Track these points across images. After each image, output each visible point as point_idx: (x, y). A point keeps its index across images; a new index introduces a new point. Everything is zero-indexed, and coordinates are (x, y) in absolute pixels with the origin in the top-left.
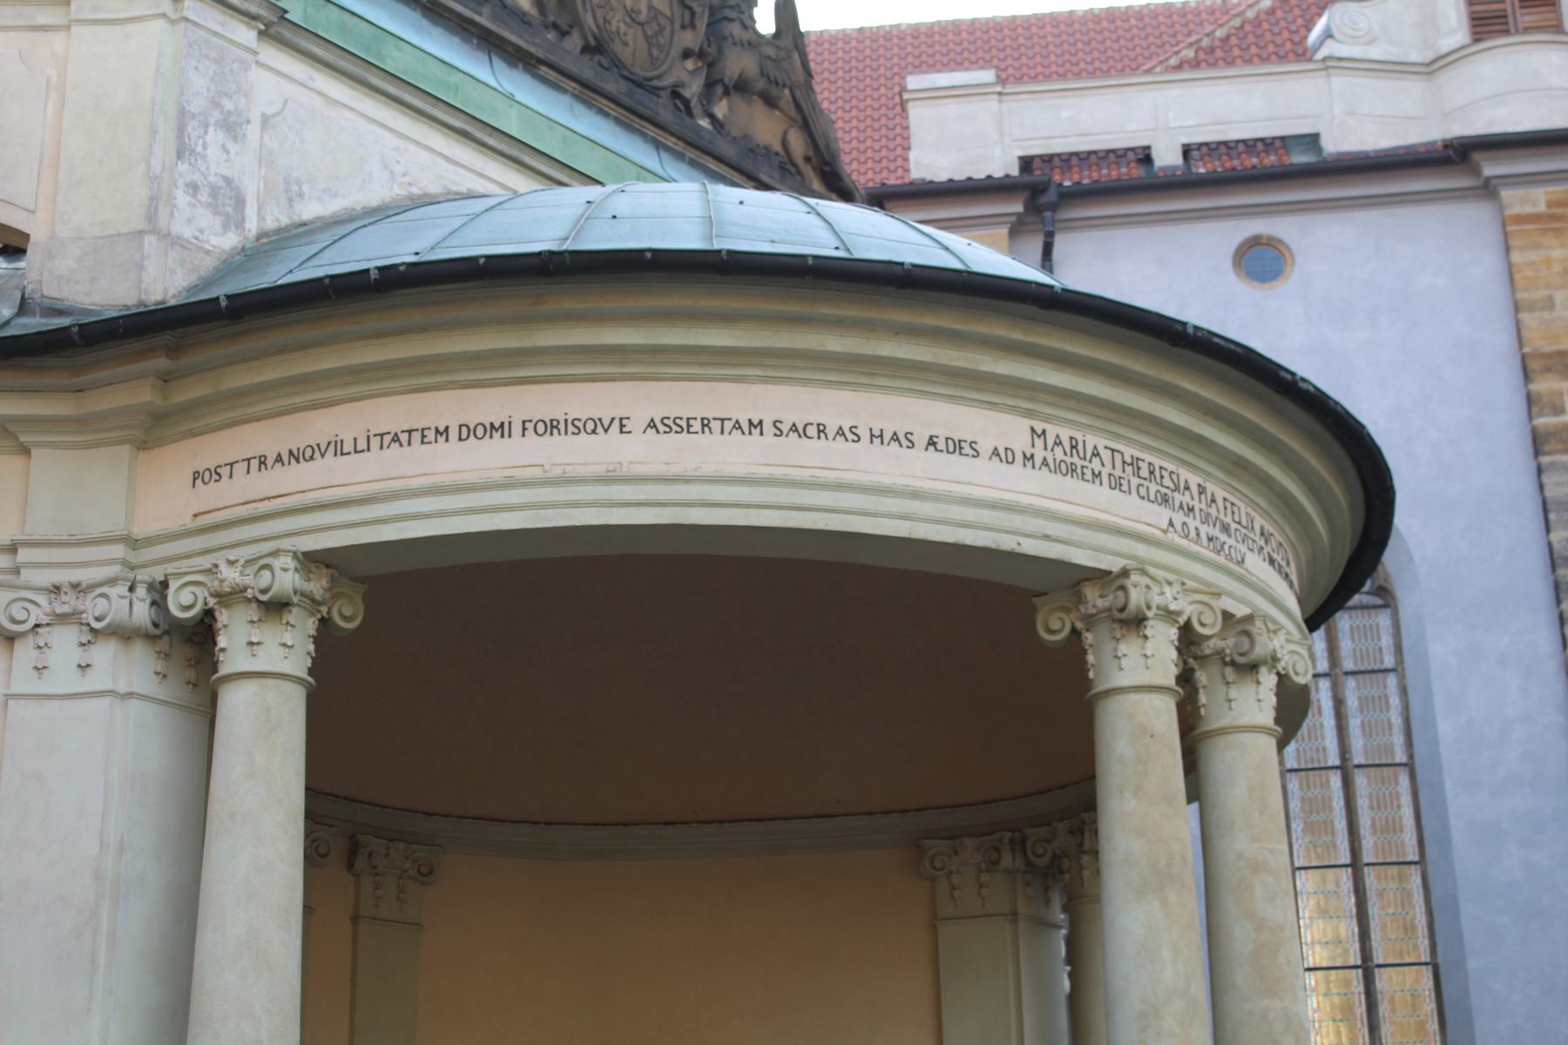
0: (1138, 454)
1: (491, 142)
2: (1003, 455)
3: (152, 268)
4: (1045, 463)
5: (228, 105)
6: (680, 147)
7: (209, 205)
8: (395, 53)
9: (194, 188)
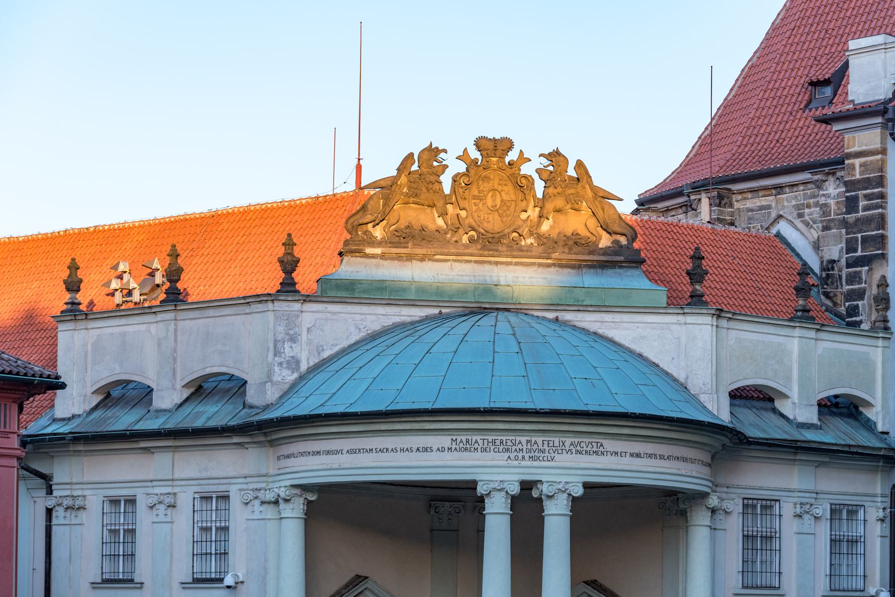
0: (494, 438)
1: (401, 303)
2: (441, 450)
3: (269, 393)
4: (456, 449)
5: (291, 332)
6: (509, 260)
7: (287, 367)
8: (359, 286)
9: (281, 364)
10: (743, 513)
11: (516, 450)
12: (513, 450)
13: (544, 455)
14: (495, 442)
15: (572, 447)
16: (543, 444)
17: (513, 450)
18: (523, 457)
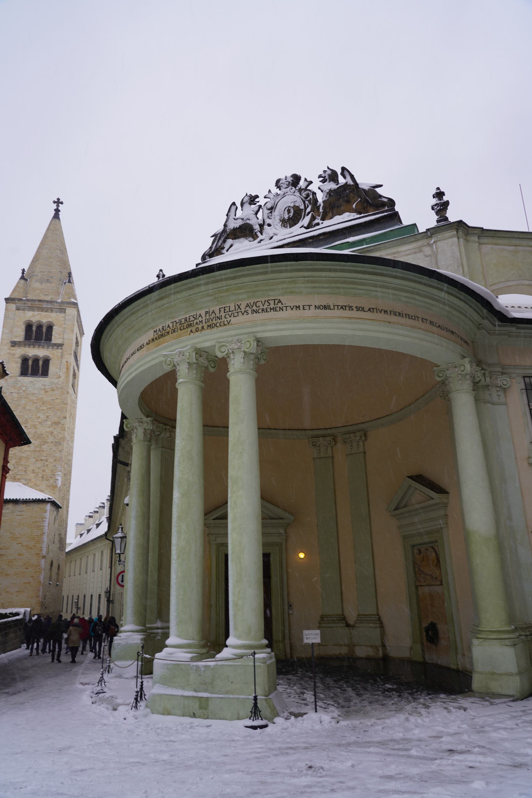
0: (180, 318)
10: (526, 389)
11: (197, 323)
12: (195, 324)
13: (221, 321)
14: (181, 322)
15: (248, 308)
16: (220, 311)
17: (195, 324)
18: (203, 327)
